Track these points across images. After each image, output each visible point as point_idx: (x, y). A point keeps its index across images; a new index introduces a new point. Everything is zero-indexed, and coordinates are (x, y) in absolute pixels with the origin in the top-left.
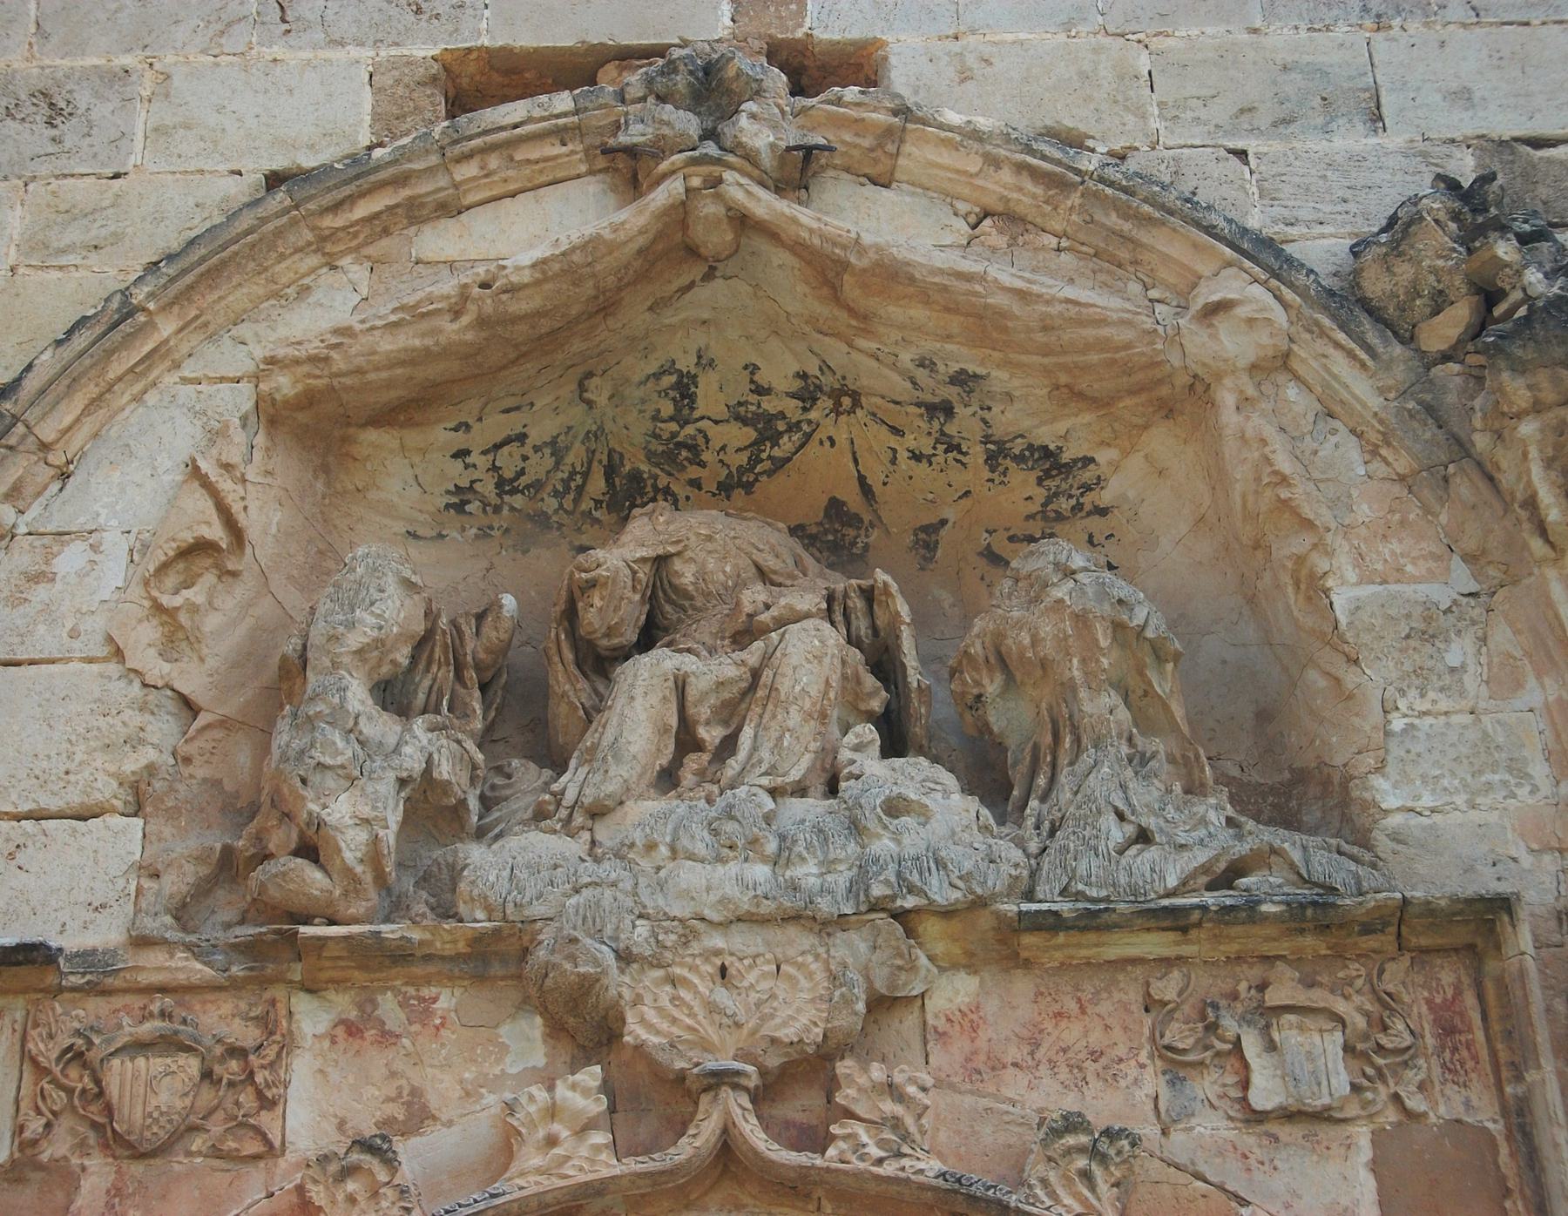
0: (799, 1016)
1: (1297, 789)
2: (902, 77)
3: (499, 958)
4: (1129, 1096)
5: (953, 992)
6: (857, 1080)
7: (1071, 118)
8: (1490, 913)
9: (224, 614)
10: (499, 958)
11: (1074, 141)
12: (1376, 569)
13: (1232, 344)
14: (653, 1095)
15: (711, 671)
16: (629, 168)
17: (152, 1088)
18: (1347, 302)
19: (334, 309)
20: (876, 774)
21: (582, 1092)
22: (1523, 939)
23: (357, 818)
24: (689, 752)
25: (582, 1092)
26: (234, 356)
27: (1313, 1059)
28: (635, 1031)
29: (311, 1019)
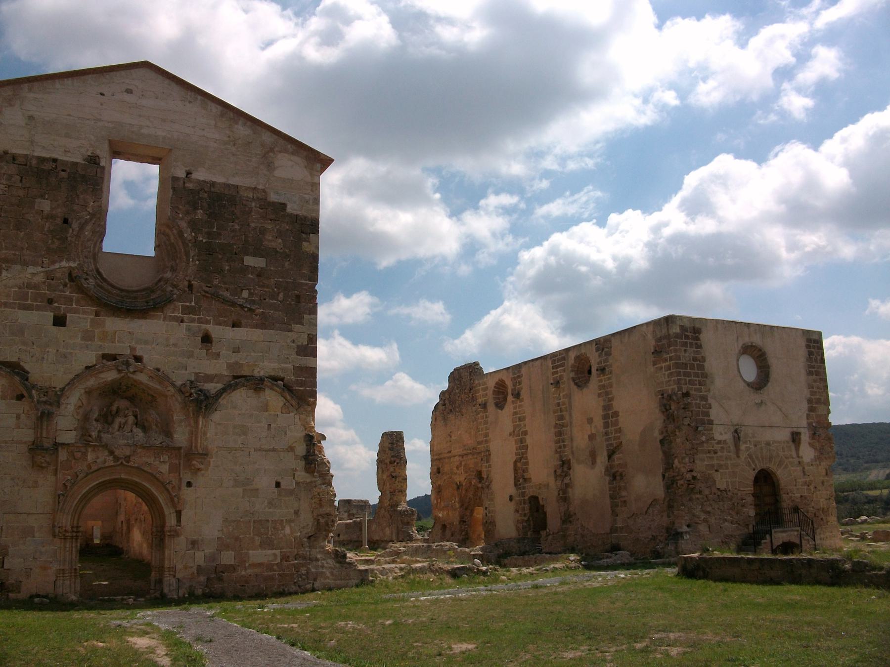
0: (128, 453)
1: (168, 434)
2: (145, 360)
3: (105, 446)
4: (151, 460)
5: (139, 450)
6: (132, 458)
7: (159, 366)
8: (180, 448)
9: (81, 411)
10: (105, 446)
11: (158, 370)
12: (178, 416)
14: (116, 459)
15: (123, 420)
16: (119, 371)
17: (78, 455)
19: (92, 382)
20: (135, 430)
21: (111, 458)
22: (182, 451)
25: (111, 458)
27: (166, 458)
28: (116, 453)
29: (90, 449)
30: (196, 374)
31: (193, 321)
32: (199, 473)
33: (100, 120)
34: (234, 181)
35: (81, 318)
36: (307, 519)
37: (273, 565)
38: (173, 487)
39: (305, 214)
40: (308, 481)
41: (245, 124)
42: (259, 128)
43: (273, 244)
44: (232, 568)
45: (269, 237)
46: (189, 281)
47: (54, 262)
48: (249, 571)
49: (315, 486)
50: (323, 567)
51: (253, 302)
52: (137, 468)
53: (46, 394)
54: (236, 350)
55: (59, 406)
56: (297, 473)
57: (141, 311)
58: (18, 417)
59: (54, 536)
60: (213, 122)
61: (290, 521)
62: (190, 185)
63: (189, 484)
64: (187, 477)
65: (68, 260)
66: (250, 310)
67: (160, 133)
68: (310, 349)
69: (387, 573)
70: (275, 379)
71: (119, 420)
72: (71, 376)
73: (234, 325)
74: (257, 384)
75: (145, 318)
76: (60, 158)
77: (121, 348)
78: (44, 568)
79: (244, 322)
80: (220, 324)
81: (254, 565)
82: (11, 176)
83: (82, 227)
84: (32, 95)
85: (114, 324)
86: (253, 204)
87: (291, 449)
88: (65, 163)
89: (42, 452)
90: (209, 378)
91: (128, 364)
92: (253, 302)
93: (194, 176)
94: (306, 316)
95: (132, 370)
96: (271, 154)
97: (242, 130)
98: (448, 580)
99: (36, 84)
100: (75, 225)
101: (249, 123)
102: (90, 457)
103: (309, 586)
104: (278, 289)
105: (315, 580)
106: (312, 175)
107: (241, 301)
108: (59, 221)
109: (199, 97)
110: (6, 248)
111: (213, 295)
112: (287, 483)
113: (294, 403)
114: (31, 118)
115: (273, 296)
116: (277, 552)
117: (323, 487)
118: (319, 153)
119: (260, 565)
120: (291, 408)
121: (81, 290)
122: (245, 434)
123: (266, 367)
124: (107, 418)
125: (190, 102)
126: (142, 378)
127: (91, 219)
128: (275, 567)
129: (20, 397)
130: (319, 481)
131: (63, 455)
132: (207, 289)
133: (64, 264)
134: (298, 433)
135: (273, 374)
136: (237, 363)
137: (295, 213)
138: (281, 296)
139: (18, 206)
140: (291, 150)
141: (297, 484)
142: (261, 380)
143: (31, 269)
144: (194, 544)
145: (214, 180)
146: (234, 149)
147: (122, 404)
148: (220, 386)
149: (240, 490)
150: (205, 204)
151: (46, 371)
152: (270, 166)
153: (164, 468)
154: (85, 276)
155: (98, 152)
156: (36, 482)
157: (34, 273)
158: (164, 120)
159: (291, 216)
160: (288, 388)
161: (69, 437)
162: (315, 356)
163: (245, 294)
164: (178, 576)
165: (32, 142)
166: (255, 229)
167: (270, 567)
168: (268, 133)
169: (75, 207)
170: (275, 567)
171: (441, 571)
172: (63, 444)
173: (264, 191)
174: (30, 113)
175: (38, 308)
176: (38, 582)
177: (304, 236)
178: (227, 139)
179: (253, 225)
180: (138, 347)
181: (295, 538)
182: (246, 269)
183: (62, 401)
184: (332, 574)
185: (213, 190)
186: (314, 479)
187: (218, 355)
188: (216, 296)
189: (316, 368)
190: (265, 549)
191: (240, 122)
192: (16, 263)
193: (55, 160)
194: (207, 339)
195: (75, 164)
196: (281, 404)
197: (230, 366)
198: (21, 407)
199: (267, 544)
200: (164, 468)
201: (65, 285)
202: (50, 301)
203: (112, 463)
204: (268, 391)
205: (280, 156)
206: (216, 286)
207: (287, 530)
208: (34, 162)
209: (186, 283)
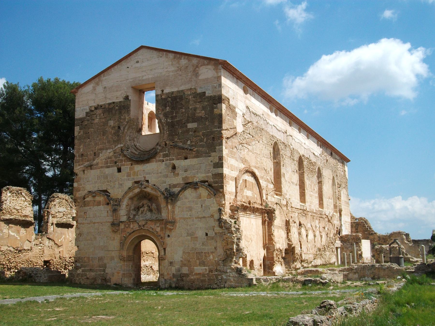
8: (163, 220)
11: (155, 185)
12: (163, 205)
13: (159, 195)
18: (163, 194)
19: (131, 194)
21: (138, 226)
23: (132, 216)
24: (142, 213)
26: (128, 197)
30: (170, 185)
31: (167, 160)
32: (172, 231)
33: (128, 79)
34: (181, 88)
35: (126, 167)
36: (220, 251)
37: (205, 274)
38: (161, 238)
39: (215, 94)
40: (221, 232)
41: (184, 58)
42: (191, 58)
43: (200, 114)
44: (187, 275)
45: (198, 111)
46: (165, 142)
47: (116, 146)
48: (195, 277)
49: (225, 234)
50: (229, 276)
51: (193, 146)
52: (147, 230)
53: (116, 201)
54: (186, 171)
55: (120, 206)
56: (215, 228)
57: (146, 160)
58: (108, 212)
59: (121, 260)
60: (171, 63)
61: (212, 253)
62: (163, 97)
63: (169, 236)
64: (168, 233)
65: (120, 144)
66: (190, 150)
67: (150, 76)
68: (219, 164)
69: (268, 281)
70: (204, 182)
71: (142, 209)
72: (124, 193)
73: (186, 158)
74: (194, 185)
75: (148, 163)
76: (115, 101)
77: (140, 178)
78: (118, 273)
79: (189, 156)
80: (179, 160)
81: (196, 274)
82: (100, 114)
83: (124, 129)
84: (105, 78)
85: (138, 168)
86: (190, 97)
87: (212, 216)
88: (117, 103)
89: (115, 225)
90: (175, 186)
91: (142, 185)
92: (193, 146)
93: (164, 92)
94: (217, 147)
95: (143, 187)
96: (197, 69)
97: (184, 62)
98: (299, 286)
99: (106, 73)
100: (122, 129)
101: (186, 57)
102: (131, 226)
103: (222, 286)
104: (203, 136)
105: (226, 283)
106: (217, 72)
107: (186, 147)
108: (117, 128)
109: (165, 53)
110: (101, 144)
111: (174, 146)
112: (211, 233)
113: (212, 193)
114: (105, 88)
115: (201, 140)
116: (207, 268)
117: (229, 234)
118: (218, 60)
119: (199, 274)
120: (211, 195)
121: (125, 156)
122: (191, 210)
123: (199, 177)
124: (137, 209)
125: (161, 57)
126: (148, 190)
127: (127, 124)
128: (206, 275)
129: (108, 204)
130: (226, 231)
131: (122, 226)
132: (172, 144)
133: (119, 146)
134: (215, 208)
135: (202, 179)
136: (186, 177)
137: (210, 95)
138: (205, 139)
139: (103, 126)
140: (206, 63)
141: (216, 233)
142: (197, 183)
143: (109, 151)
144: (171, 263)
145: (173, 90)
146: (180, 73)
147: (145, 202)
148: (179, 189)
149: (189, 238)
150: (170, 104)
151: (116, 192)
152: (196, 74)
153: (158, 229)
154: (126, 149)
155: (128, 94)
156: (114, 238)
157: (109, 153)
158: (151, 70)
159: (208, 97)
160: (209, 185)
161: (124, 219)
162: (222, 167)
163: (189, 142)
164: (166, 278)
165: (106, 98)
166: (191, 109)
167: (204, 275)
168: (195, 59)
169: (122, 121)
170: (206, 275)
171: (298, 282)
172: (121, 222)
173: (195, 89)
174: (104, 86)
175: (112, 166)
176: (115, 279)
177: (215, 106)
178: (177, 69)
179: (190, 107)
180: (147, 176)
181: (215, 261)
182: (188, 131)
183: (121, 204)
184: (234, 280)
185: (173, 96)
186: (223, 231)
187: (178, 174)
188: (175, 146)
189: (223, 174)
190: (201, 266)
191: (183, 58)
192: (104, 150)
193: (114, 103)
194: (174, 167)
195: (120, 102)
196: (207, 194)
197: (183, 179)
198: (109, 208)
199: (203, 264)
200: (158, 229)
201: (120, 155)
202: (116, 163)
203: (138, 229)
204: (201, 189)
205: (201, 68)
206: (176, 141)
207: (211, 257)
208: (107, 106)
209: (164, 143)
